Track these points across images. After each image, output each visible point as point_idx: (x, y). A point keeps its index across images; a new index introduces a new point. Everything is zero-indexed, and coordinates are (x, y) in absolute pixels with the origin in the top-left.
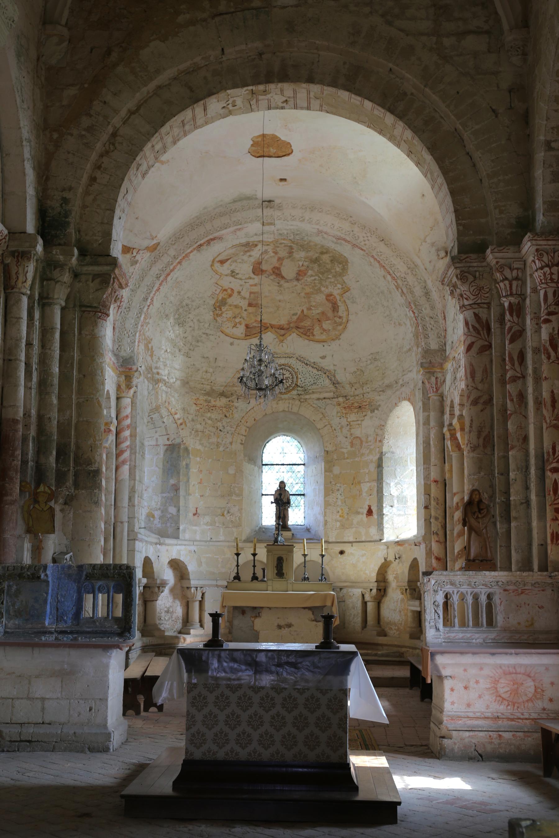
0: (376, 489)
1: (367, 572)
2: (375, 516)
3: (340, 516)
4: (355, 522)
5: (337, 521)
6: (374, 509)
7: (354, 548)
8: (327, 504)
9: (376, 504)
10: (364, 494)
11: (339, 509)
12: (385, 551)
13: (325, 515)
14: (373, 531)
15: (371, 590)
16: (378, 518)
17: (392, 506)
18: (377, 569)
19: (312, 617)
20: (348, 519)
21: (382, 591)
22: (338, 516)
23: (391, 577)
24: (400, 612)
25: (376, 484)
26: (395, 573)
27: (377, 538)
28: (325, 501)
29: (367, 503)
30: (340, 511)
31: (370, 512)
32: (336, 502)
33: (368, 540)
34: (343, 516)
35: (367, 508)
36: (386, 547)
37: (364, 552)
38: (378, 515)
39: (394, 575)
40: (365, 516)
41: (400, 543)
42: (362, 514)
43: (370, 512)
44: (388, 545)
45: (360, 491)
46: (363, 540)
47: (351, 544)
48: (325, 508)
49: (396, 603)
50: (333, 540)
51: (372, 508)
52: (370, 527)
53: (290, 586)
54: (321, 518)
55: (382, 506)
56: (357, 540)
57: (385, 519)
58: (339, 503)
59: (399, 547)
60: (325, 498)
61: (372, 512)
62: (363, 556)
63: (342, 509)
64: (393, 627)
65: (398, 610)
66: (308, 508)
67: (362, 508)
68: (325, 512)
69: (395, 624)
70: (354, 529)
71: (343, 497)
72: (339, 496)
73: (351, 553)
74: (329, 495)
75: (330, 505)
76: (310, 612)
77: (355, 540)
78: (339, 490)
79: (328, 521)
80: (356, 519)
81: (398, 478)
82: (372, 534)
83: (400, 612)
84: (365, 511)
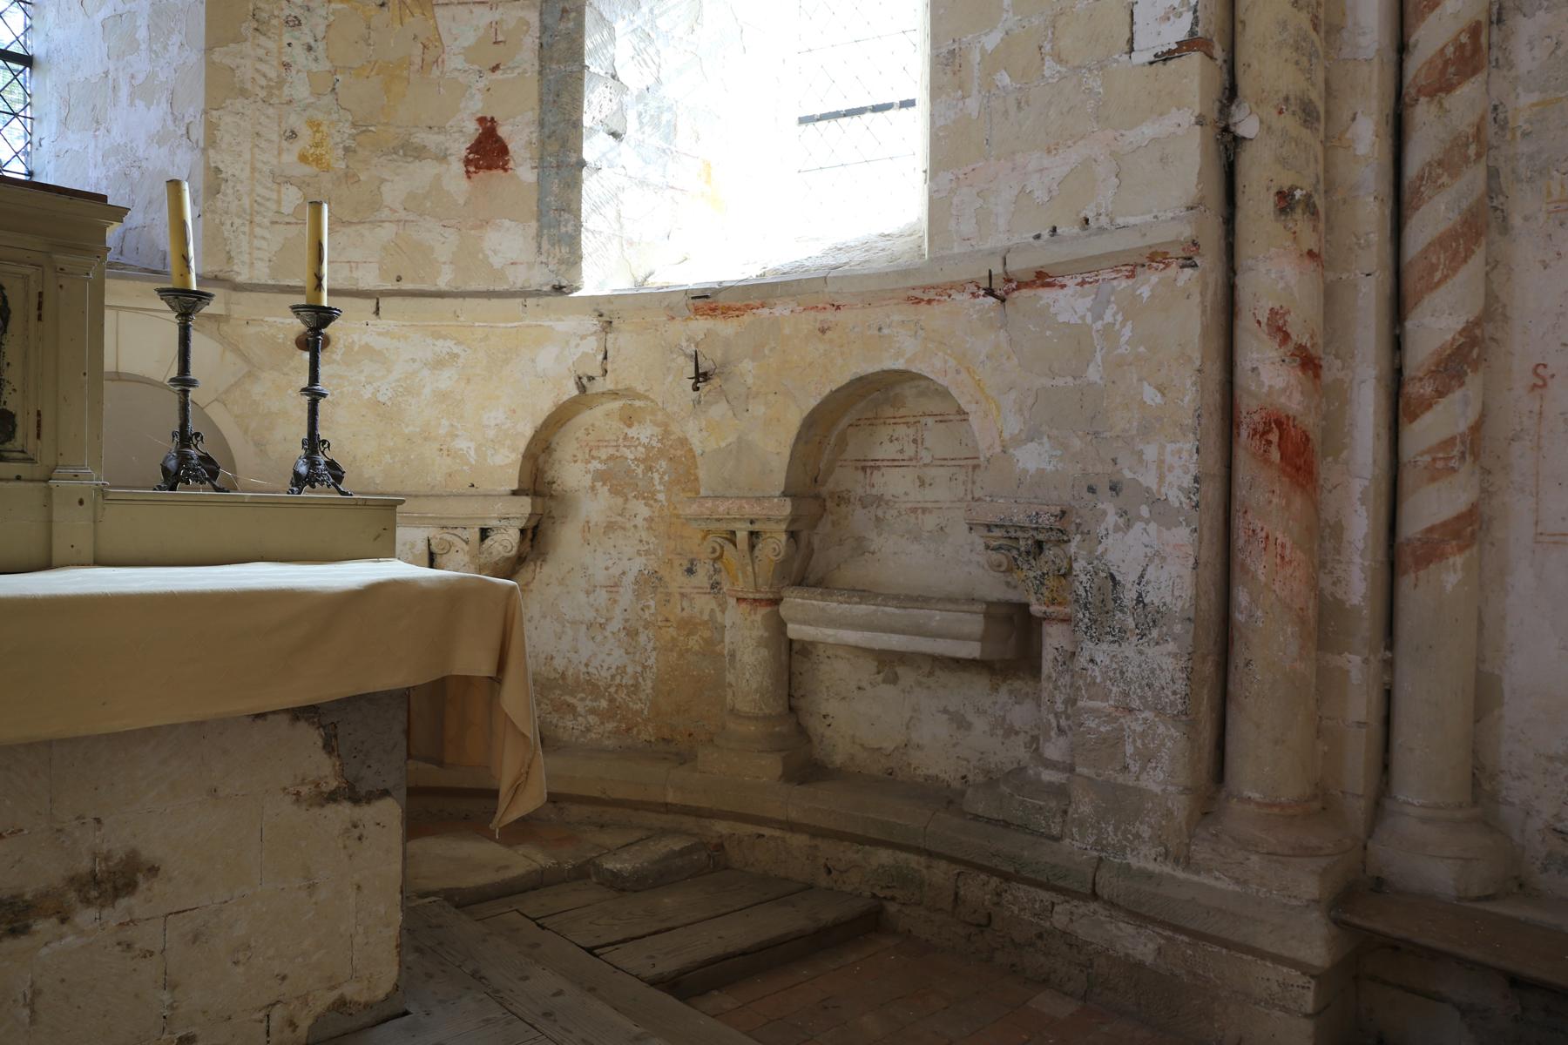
0: (530, 42)
1: (462, 444)
2: (524, 170)
3: (303, 158)
4: (395, 191)
5: (281, 179)
6: (518, 135)
7: (384, 323)
8: (222, 86)
9: (532, 115)
10: (454, 62)
11: (294, 121)
12: (591, 345)
13: (211, 142)
14: (509, 247)
15: (484, 533)
16: (540, 181)
17: (615, 135)
18: (528, 432)
19: (324, 769)
20: (349, 177)
21: (529, 535)
22: (290, 157)
23: (572, 472)
24: (632, 633)
25: (533, 18)
26: (603, 454)
27: (540, 278)
28: (210, 64)
29: (476, 105)
30: (305, 133)
31: (488, 151)
32: (281, 83)
33: (473, 286)
34: (318, 160)
35: (472, 129)
36: (591, 323)
37: (444, 346)
38: (541, 166)
39: (595, 465)
40: (458, 167)
41: (722, 301)
42: (443, 158)
43: (488, 151)
44: (607, 313)
45: (432, 48)
46: (442, 284)
47: (371, 304)
48: (213, 104)
49: (602, 596)
50: (262, 274)
51: (503, 131)
52: (484, 223)
53: (72, 525)
54: (183, 163)
55: (577, 125)
56: (406, 286)
57: (592, 188)
58: (300, 90)
59: (701, 325)
60: (209, 49)
61: (504, 150)
62: (439, 364)
63: (315, 126)
64: (581, 703)
65: (615, 625)
66: (64, 122)
67: (442, 130)
68: (211, 127)
69: (594, 689)
70: (387, 232)
71: (326, 65)
72: (299, 56)
73: (368, 350)
74: (239, 39)
75: (243, 93)
76: (311, 736)
77: (389, 286)
78: (297, 23)
79: (228, 171)
80: (400, 183)
81: (645, 9)
82: (497, 261)
83: (632, 633)
84: (460, 147)
